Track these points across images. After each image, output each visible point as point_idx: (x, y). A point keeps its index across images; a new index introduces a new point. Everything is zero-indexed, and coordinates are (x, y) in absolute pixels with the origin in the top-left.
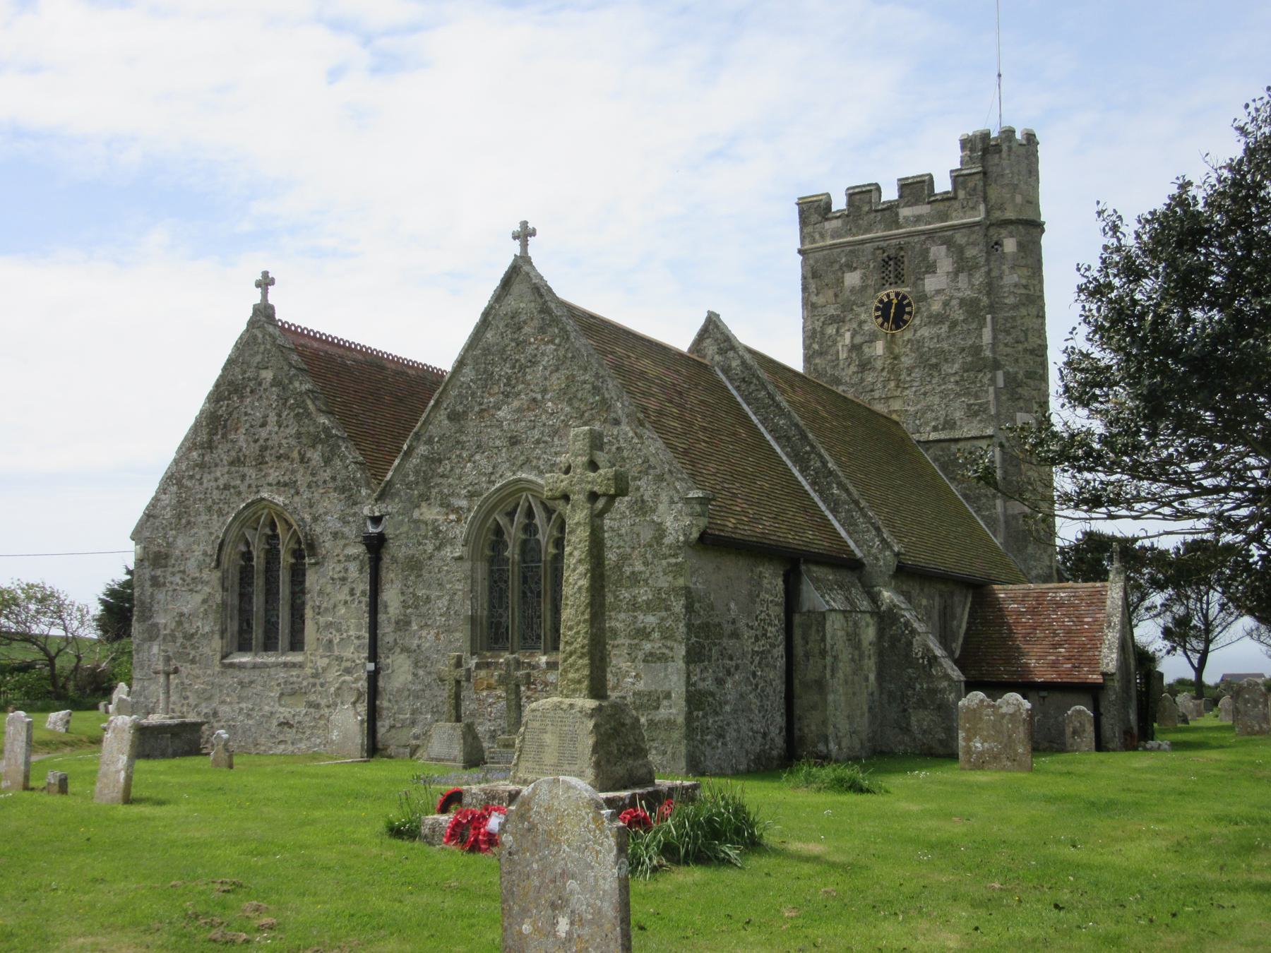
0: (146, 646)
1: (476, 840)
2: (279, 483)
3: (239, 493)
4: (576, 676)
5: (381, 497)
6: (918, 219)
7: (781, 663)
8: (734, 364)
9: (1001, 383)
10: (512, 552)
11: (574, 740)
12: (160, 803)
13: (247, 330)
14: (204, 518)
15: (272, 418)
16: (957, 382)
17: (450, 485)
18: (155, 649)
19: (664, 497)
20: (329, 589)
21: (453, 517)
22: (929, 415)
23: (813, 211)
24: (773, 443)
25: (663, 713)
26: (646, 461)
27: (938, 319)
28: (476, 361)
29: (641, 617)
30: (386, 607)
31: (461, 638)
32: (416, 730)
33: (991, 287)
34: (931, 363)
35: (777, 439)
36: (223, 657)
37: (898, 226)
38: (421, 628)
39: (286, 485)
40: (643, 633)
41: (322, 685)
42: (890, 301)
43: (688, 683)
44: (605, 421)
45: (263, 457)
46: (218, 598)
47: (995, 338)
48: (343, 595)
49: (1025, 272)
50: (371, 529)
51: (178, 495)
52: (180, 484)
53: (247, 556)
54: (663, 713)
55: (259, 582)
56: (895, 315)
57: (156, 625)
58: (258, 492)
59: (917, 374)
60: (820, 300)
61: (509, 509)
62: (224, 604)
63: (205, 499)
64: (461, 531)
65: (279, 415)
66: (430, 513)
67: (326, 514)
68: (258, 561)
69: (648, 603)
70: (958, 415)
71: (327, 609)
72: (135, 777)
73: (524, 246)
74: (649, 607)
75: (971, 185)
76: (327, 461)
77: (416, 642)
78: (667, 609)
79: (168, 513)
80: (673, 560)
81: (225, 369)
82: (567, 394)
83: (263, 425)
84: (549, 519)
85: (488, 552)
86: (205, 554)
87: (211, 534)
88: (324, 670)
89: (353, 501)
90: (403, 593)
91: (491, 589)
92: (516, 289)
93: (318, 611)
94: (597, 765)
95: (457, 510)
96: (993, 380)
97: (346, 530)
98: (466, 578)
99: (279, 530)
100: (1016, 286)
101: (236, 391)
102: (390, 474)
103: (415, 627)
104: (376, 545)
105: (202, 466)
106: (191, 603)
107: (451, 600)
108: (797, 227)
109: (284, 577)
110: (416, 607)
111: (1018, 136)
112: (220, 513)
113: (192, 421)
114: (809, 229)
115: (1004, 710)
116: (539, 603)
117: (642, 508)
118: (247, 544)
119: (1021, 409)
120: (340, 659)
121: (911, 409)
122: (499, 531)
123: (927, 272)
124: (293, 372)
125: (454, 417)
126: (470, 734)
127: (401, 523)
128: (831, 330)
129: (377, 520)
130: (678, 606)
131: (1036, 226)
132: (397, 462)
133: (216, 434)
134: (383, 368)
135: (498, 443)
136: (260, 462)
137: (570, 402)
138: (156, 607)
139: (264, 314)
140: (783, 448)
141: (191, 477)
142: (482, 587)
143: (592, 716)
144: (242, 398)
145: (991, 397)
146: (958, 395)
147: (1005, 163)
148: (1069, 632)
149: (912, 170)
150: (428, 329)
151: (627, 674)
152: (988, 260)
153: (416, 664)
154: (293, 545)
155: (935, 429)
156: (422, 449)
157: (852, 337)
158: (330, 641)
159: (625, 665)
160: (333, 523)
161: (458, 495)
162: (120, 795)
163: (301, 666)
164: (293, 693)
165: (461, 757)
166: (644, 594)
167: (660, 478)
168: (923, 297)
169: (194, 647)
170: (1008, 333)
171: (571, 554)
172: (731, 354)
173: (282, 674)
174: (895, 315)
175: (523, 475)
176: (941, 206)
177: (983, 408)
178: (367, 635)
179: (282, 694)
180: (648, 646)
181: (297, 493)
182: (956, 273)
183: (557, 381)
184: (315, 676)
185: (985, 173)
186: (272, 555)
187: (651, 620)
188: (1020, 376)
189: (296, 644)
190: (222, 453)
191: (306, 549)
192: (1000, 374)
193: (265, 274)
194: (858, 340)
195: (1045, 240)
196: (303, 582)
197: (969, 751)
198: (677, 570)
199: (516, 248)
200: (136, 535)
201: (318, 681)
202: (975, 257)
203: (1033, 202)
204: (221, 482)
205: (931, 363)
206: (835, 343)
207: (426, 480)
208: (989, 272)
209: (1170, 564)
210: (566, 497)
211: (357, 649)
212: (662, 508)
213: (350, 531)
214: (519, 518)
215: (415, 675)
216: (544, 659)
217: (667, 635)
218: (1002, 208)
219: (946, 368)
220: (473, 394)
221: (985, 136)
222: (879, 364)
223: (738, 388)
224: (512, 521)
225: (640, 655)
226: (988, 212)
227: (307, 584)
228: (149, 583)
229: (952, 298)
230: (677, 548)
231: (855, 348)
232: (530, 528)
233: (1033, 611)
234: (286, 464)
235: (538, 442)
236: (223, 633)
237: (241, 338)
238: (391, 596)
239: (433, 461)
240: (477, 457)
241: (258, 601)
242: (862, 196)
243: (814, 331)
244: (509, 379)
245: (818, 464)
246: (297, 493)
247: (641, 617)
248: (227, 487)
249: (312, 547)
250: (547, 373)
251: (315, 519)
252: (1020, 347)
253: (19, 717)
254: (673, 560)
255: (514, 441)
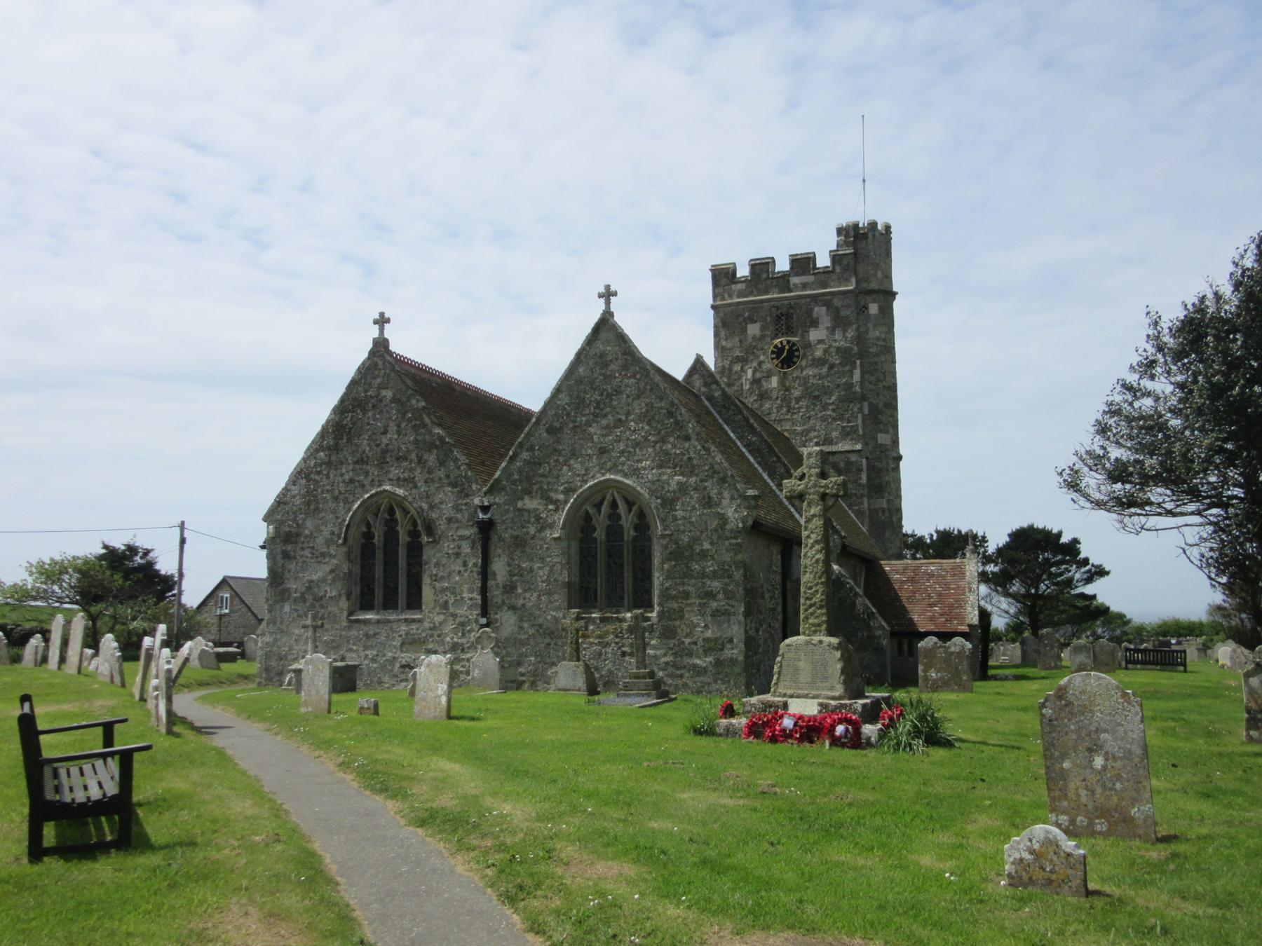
0: (278, 606)
1: (774, 735)
2: (399, 479)
3: (363, 486)
4: (816, 621)
5: (490, 491)
6: (805, 286)
7: (780, 617)
8: (717, 394)
9: (866, 411)
10: (600, 534)
11: (825, 666)
12: (473, 719)
13: (369, 358)
14: (332, 505)
15: (393, 427)
16: (833, 410)
17: (548, 483)
18: (287, 608)
19: (726, 494)
20: (444, 561)
21: (551, 507)
22: (813, 434)
23: (723, 277)
24: (747, 454)
25: (729, 653)
26: (712, 466)
27: (819, 362)
28: (569, 387)
29: (708, 583)
30: (495, 575)
31: (560, 599)
32: (522, 670)
33: (860, 339)
34: (815, 396)
35: (750, 452)
36: (350, 614)
37: (790, 291)
38: (525, 591)
39: (405, 480)
40: (710, 595)
41: (439, 636)
42: (783, 347)
43: (746, 631)
44: (678, 437)
45: (384, 458)
46: (345, 567)
47: (862, 377)
48: (457, 566)
49: (885, 329)
50: (481, 516)
51: (307, 486)
52: (308, 478)
53: (368, 536)
54: (729, 653)
55: (379, 555)
56: (787, 358)
57: (287, 590)
58: (380, 485)
59: (803, 403)
60: (728, 345)
61: (597, 501)
62: (350, 573)
63: (332, 491)
64: (561, 518)
65: (399, 426)
66: (530, 503)
67: (441, 503)
68: (378, 539)
69: (714, 572)
70: (834, 434)
71: (442, 577)
72: (453, 703)
73: (608, 303)
74: (714, 576)
75: (845, 262)
76: (442, 463)
77: (521, 602)
78: (730, 577)
79: (298, 501)
80: (734, 541)
81: (349, 388)
82: (644, 417)
83: (385, 432)
84: (630, 511)
85: (580, 535)
86: (332, 533)
87: (338, 518)
88: (441, 624)
89: (465, 493)
90: (509, 565)
91: (581, 562)
92: (603, 336)
93: (435, 578)
94: (845, 683)
95: (556, 502)
96: (861, 409)
97: (459, 516)
98: (563, 553)
99: (398, 515)
100: (878, 339)
101: (359, 406)
102: (498, 474)
103: (520, 590)
104: (486, 529)
105: (329, 464)
106: (318, 572)
107: (551, 571)
108: (710, 287)
109: (402, 553)
110: (522, 575)
111: (879, 227)
112: (346, 501)
113: (319, 428)
114: (720, 290)
115: (952, 649)
116: (622, 573)
117: (708, 502)
118: (368, 525)
119: (881, 431)
120: (454, 616)
121: (799, 429)
122: (588, 518)
123: (811, 326)
124: (410, 392)
125: (551, 431)
126: (588, 670)
127: (507, 511)
128: (737, 368)
129: (485, 509)
130: (738, 575)
131: (892, 295)
132: (504, 464)
133: (342, 439)
134: (454, 390)
135: (589, 451)
136: (382, 463)
137: (649, 424)
138: (287, 575)
139: (381, 346)
140: (755, 458)
141: (319, 473)
142: (575, 560)
143: (837, 649)
144: (365, 411)
145: (860, 421)
146: (835, 419)
147: (871, 247)
148: (940, 595)
149: (802, 249)
150: (521, 366)
151: (698, 625)
152: (857, 319)
153: (521, 620)
154: (409, 527)
155: (817, 444)
156: (525, 455)
157: (754, 373)
158: (446, 602)
159: (695, 619)
160: (447, 509)
161: (556, 491)
162: (444, 714)
163: (419, 621)
164: (413, 642)
165: (584, 687)
166: (710, 567)
167: (723, 480)
168: (808, 346)
169: (322, 607)
170: (872, 374)
171: (808, 537)
172: (714, 386)
173: (404, 628)
174: (787, 358)
175: (608, 476)
176: (822, 277)
177: (854, 430)
178: (479, 597)
179: (403, 644)
180: (714, 604)
181: (416, 487)
182: (832, 330)
183: (638, 407)
184: (434, 628)
185: (855, 254)
186: (391, 535)
187: (716, 585)
188: (881, 405)
189: (414, 602)
190: (347, 454)
191: (422, 530)
192: (866, 404)
193: (382, 314)
194: (758, 375)
195: (897, 305)
196: (421, 556)
197: (926, 679)
198: (738, 548)
199: (600, 306)
200: (268, 518)
201: (436, 633)
202: (847, 317)
203: (888, 277)
204: (347, 477)
205: (815, 396)
206: (740, 377)
207: (529, 479)
208: (857, 329)
209: (929, 546)
210: (801, 496)
211: (470, 608)
212: (725, 502)
213: (463, 517)
214: (605, 508)
215: (521, 628)
216: (629, 615)
217: (730, 596)
218: (867, 280)
219: (825, 399)
220: (568, 415)
221: (856, 226)
222: (774, 395)
223: (719, 413)
224: (599, 512)
225: (708, 611)
226: (857, 283)
227: (424, 557)
228: (279, 557)
229: (830, 346)
230: (736, 533)
231: (756, 382)
232: (614, 516)
233: (912, 580)
234: (405, 464)
235: (623, 452)
236: (349, 596)
237: (363, 364)
238: (499, 567)
239: (534, 463)
240: (572, 462)
241: (379, 572)
242: (761, 268)
243: (724, 367)
244: (598, 403)
245: (782, 470)
246: (416, 487)
247: (708, 583)
248: (351, 481)
249: (430, 529)
250: (630, 400)
251: (432, 507)
252: (881, 385)
253: (318, 658)
254: (734, 541)
255: (603, 451)
